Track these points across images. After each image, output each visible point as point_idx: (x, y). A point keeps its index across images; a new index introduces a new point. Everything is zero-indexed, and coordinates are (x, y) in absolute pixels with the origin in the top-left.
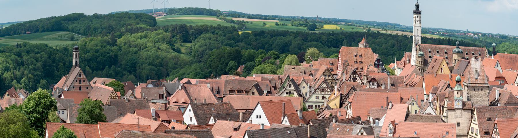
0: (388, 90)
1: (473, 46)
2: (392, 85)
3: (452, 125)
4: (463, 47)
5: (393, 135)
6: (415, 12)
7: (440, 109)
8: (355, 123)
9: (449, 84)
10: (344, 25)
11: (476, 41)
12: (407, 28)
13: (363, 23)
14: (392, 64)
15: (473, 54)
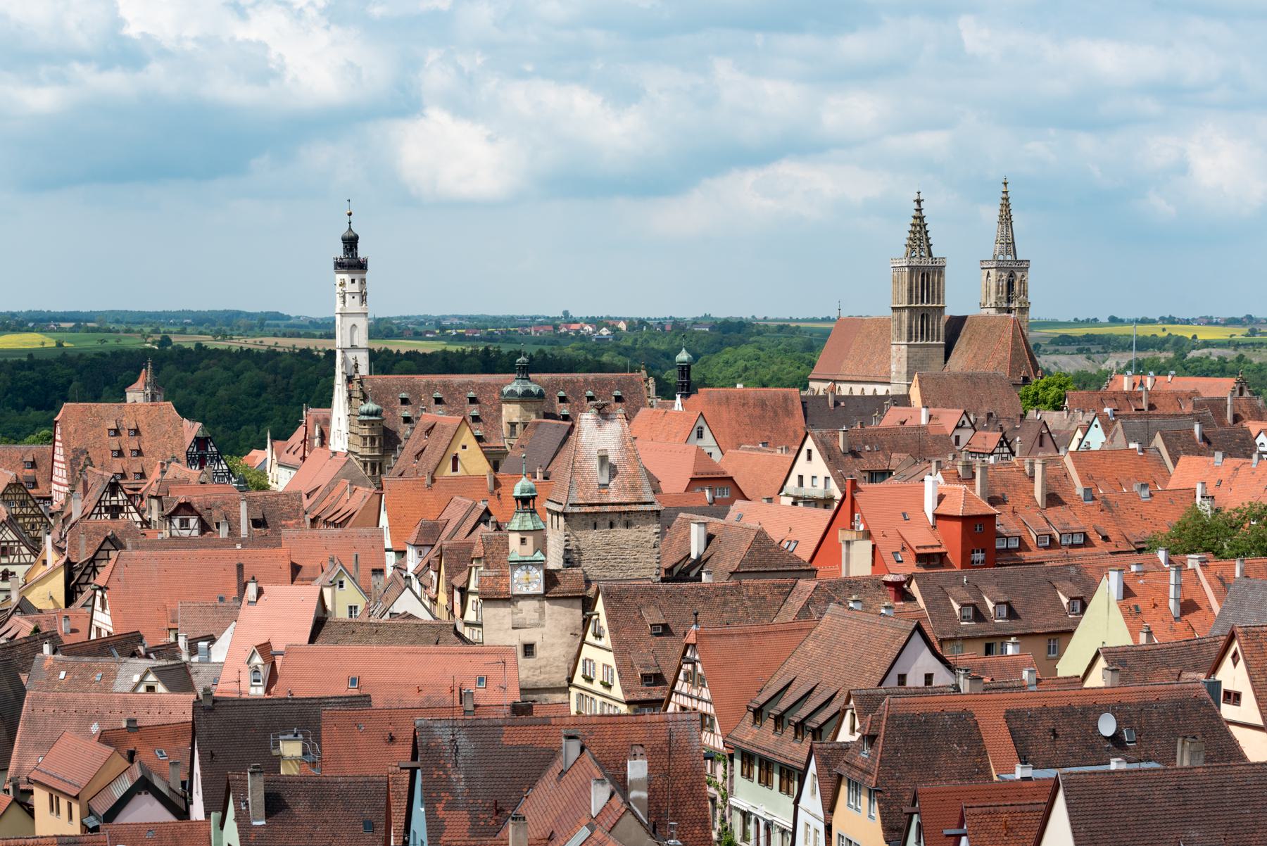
1: (590, 371)
2: (257, 523)
3: (502, 655)
5: (267, 691)
6: (340, 266)
7: (451, 599)
8: (122, 655)
9: (487, 512)
10: (72, 330)
11: (603, 351)
12: (314, 324)
13: (142, 318)
14: (254, 452)
15: (590, 398)
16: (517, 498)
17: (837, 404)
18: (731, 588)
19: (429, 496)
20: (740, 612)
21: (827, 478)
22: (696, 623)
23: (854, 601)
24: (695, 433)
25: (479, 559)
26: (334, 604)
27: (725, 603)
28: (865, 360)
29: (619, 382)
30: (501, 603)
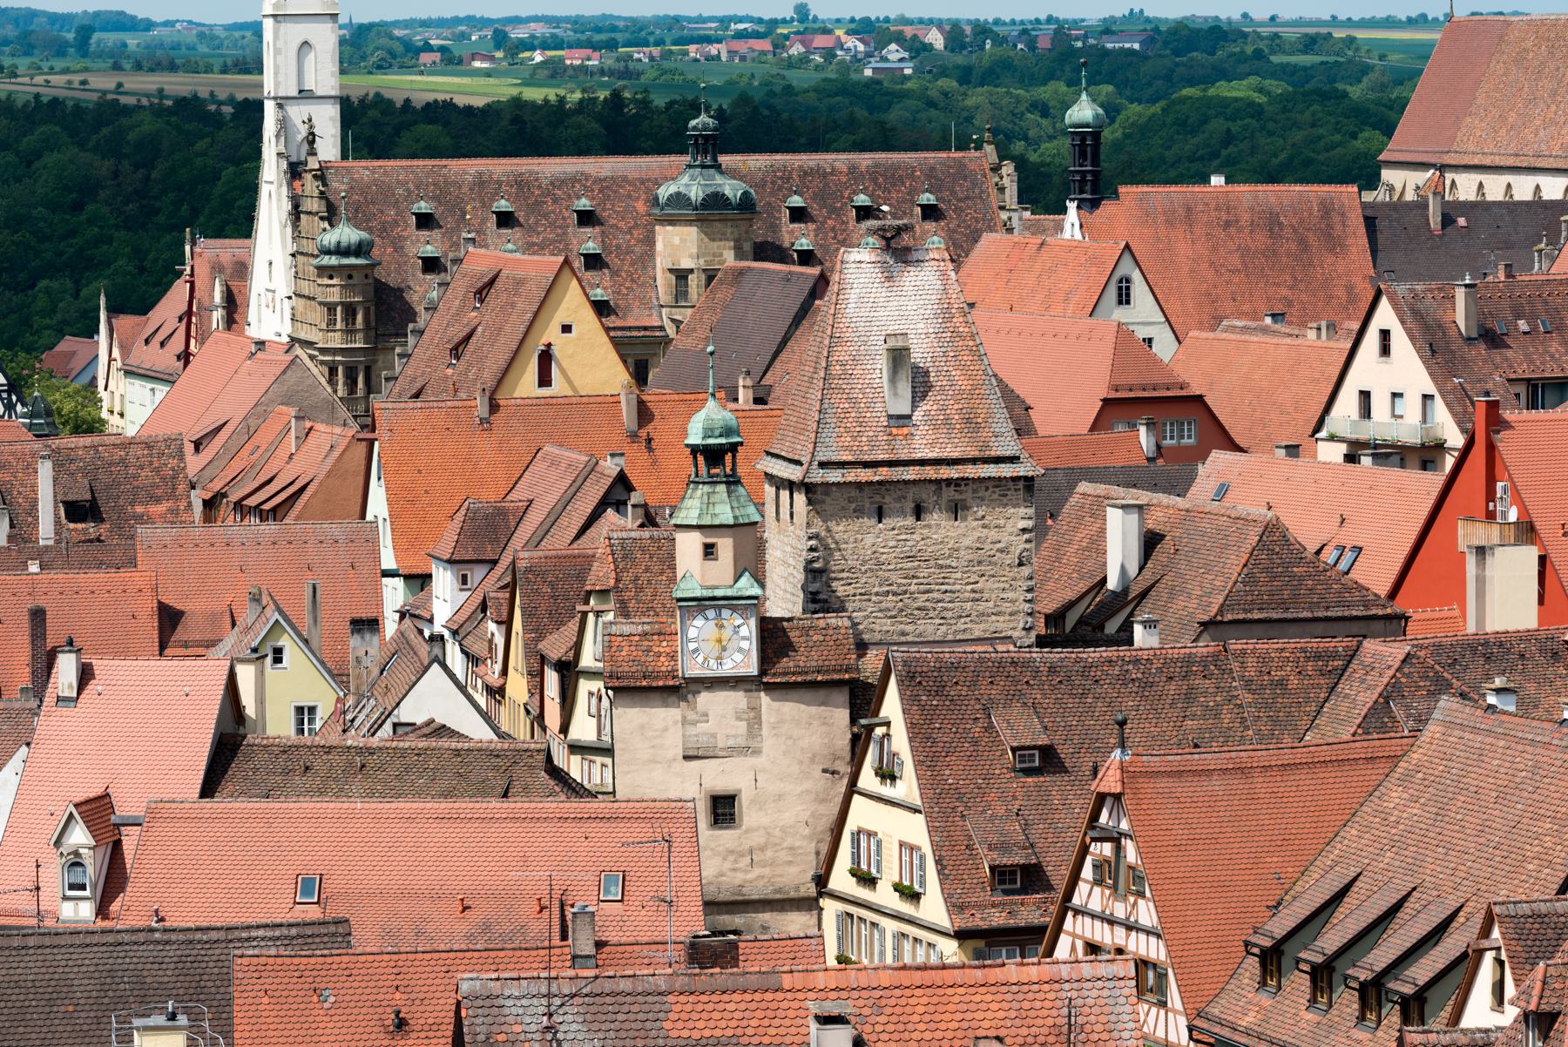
0: (41, 555)
2: (77, 511)
3: (660, 818)
4: (757, 162)
5: (102, 911)
7: (538, 689)
9: (623, 481)
14: (68, 344)
15: (864, 213)
16: (695, 450)
17: (1447, 221)
18: (1204, 661)
19: (485, 444)
20: (1226, 719)
21: (1427, 398)
22: (1123, 746)
23: (1498, 691)
24: (1112, 292)
25: (604, 593)
26: (261, 701)
27: (1189, 696)
28: (1512, 117)
29: (931, 173)
30: (656, 696)
